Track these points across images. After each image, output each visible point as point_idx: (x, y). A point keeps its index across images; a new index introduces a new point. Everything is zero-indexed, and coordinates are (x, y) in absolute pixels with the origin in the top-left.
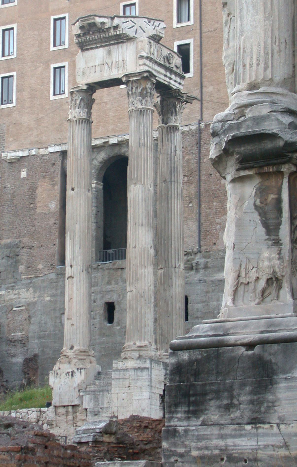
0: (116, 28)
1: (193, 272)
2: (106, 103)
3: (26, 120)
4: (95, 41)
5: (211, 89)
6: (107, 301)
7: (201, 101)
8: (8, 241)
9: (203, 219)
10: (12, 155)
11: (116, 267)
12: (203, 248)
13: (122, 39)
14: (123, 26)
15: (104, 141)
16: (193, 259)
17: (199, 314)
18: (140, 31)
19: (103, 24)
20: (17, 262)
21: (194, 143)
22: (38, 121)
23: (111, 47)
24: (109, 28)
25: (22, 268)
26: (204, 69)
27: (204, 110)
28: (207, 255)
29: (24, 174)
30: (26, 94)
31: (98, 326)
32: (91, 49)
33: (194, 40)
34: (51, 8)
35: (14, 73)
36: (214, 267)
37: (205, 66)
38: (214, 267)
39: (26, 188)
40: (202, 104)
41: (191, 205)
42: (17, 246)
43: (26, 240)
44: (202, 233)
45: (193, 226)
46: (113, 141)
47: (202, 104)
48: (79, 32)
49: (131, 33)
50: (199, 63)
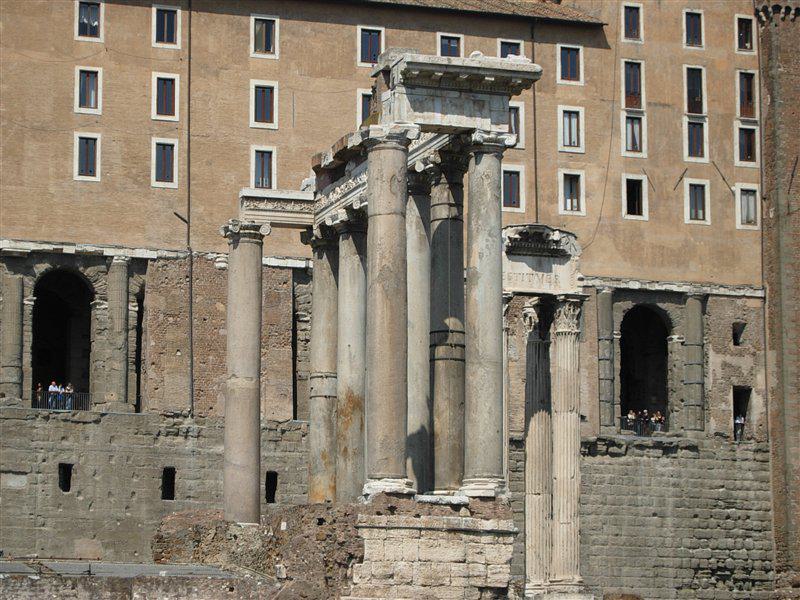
0: (557, 242)
1: (180, 439)
2: (53, 196)
4: (529, 249)
5: (201, 209)
6: (63, 461)
7: (188, 222)
9: (196, 374)
11: (76, 418)
12: (196, 412)
14: (564, 240)
15: (56, 247)
16: (181, 423)
17: (192, 493)
21: (183, 275)
23: (543, 258)
26: (192, 182)
27: (191, 234)
28: (200, 419)
31: (51, 494)
32: (519, 255)
33: (180, 142)
36: (210, 436)
37: (194, 179)
38: (210, 436)
40: (189, 227)
41: (179, 354)
44: (195, 393)
45: (186, 381)
46: (68, 250)
47: (189, 227)
48: (517, 236)
49: (566, 248)
50: (186, 174)
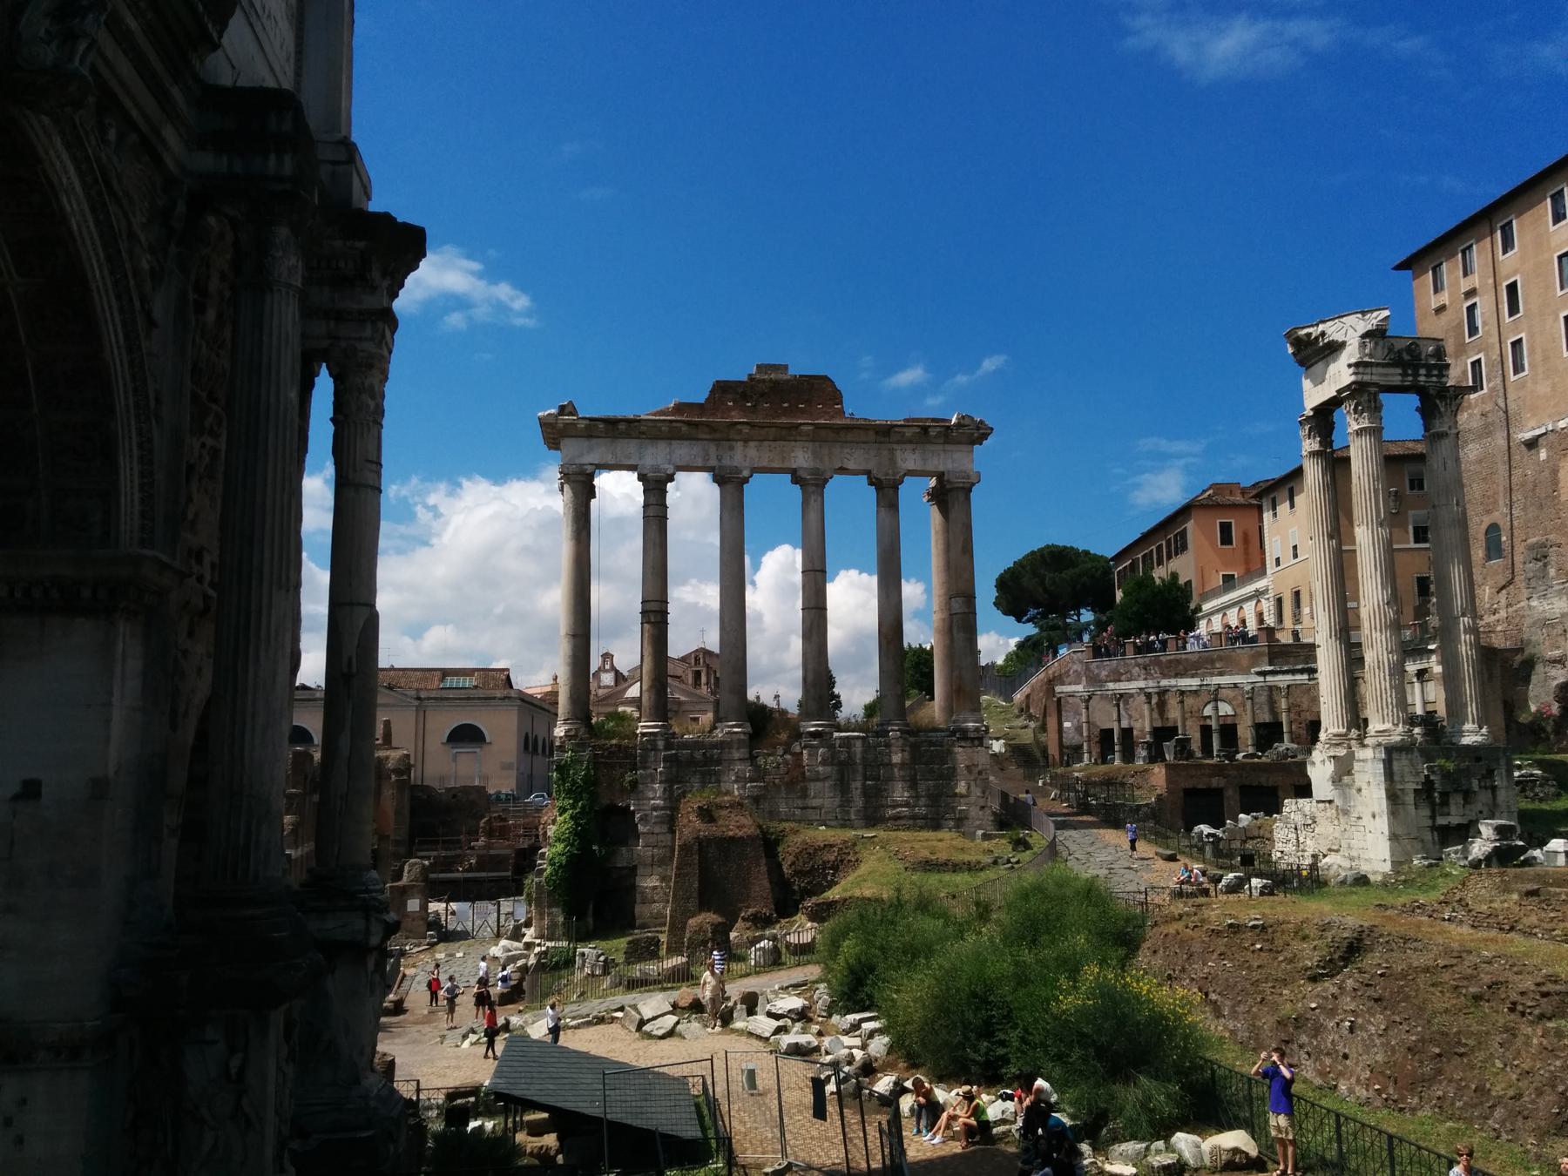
0: (1323, 334)
3: (1543, 388)
8: (1534, 540)
10: (1528, 435)
13: (1342, 345)
14: (1329, 332)
18: (1351, 331)
19: (1309, 335)
20: (1545, 565)
22: (1554, 386)
24: (1317, 338)
25: (1552, 572)
29: (1543, 455)
30: (1539, 357)
34: (1553, 244)
35: (1523, 335)
39: (1547, 473)
42: (1543, 546)
43: (1551, 537)
49: (1339, 337)
